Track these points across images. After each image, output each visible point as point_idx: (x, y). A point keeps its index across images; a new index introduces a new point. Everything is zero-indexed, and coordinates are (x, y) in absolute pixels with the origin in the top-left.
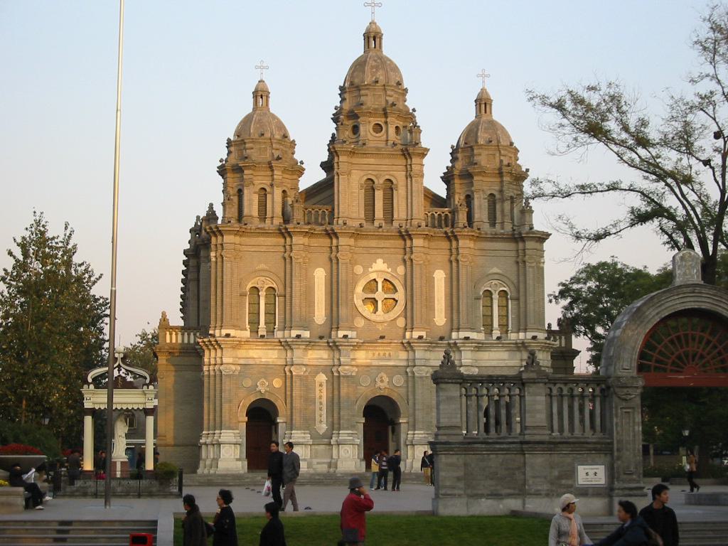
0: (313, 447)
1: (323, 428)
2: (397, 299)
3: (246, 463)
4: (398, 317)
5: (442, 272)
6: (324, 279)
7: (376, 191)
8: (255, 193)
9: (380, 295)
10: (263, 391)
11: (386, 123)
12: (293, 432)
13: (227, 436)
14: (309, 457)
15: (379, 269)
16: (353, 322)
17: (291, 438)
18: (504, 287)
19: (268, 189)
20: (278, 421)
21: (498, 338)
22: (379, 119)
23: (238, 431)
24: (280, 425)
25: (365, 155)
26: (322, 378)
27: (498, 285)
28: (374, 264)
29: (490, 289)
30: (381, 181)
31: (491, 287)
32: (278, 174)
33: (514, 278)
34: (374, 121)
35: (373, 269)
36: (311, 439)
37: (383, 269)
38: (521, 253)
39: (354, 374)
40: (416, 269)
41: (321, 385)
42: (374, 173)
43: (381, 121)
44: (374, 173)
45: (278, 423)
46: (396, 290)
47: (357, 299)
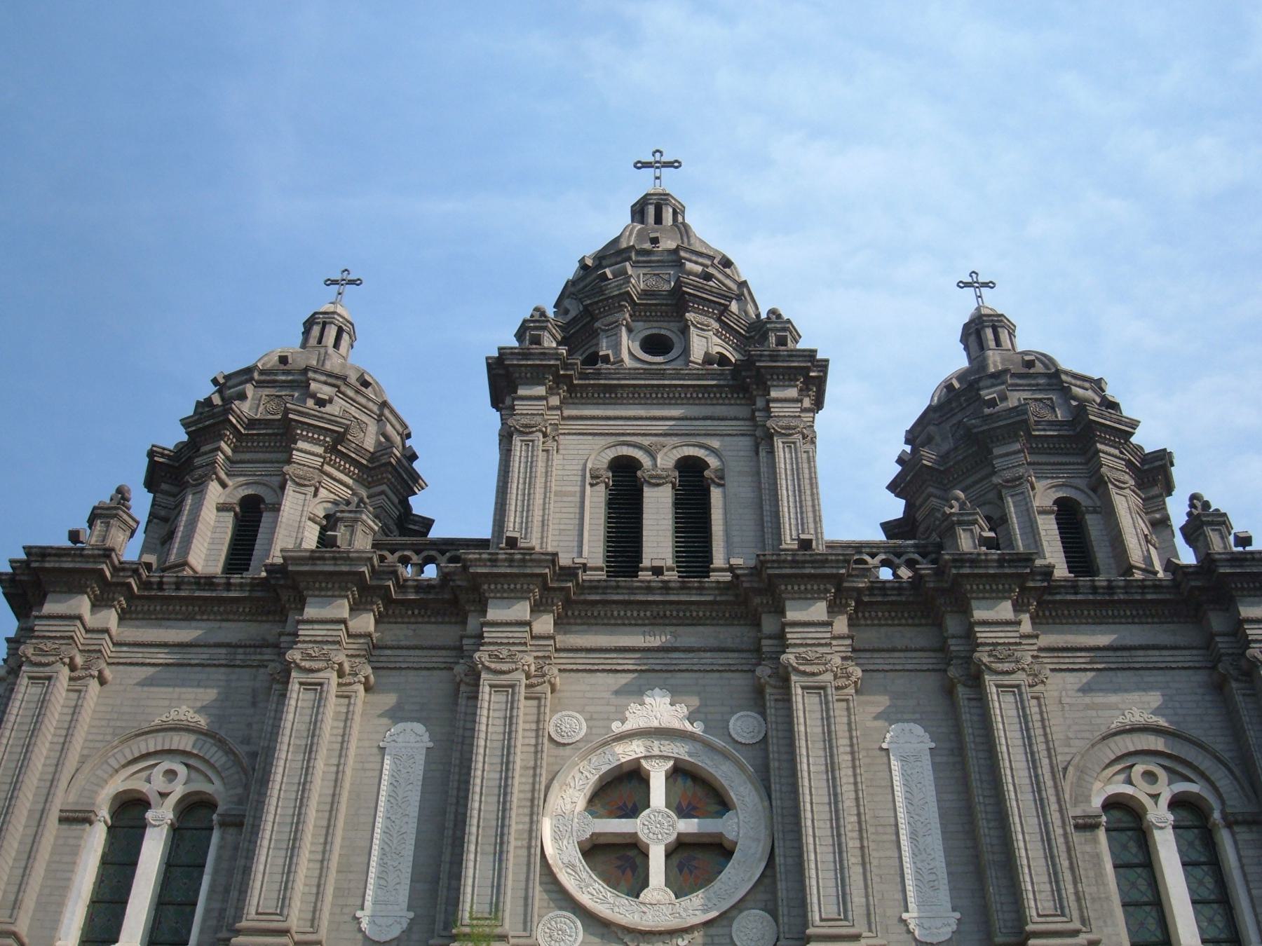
2: (731, 836)
4: (739, 907)
5: (918, 730)
6: (420, 759)
7: (646, 489)
8: (222, 508)
11: (685, 331)
15: (655, 724)
16: (526, 923)
18: (1193, 781)
19: (269, 498)
22: (665, 324)
25: (610, 394)
27: (1162, 775)
28: (633, 707)
29: (1129, 790)
30: (666, 460)
31: (1129, 781)
32: (307, 453)
33: (1220, 744)
34: (644, 330)
35: (630, 725)
37: (676, 724)
38: (1222, 643)
40: (805, 708)
42: (645, 441)
43: (666, 329)
44: (645, 441)
46: (723, 804)
47: (557, 838)
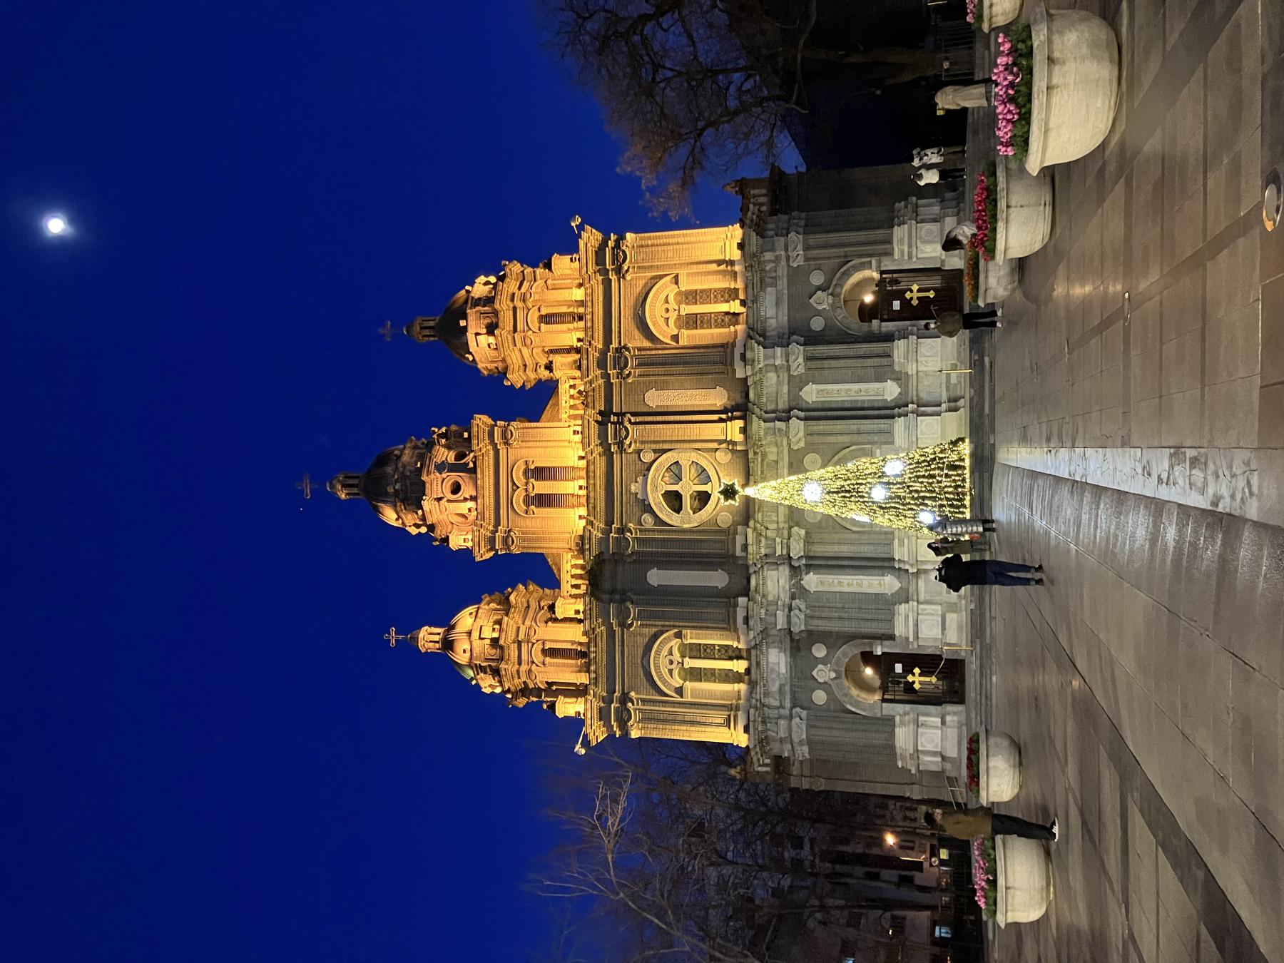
0: (922, 598)
1: (887, 584)
3: (949, 708)
9: (687, 488)
10: (833, 675)
12: (897, 634)
13: (903, 737)
14: (939, 608)
17: (907, 638)
20: (879, 653)
21: (743, 303)
23: (897, 719)
24: (886, 650)
26: (812, 581)
36: (908, 602)
39: (803, 532)
41: (822, 583)
45: (883, 653)
47: (689, 522)
